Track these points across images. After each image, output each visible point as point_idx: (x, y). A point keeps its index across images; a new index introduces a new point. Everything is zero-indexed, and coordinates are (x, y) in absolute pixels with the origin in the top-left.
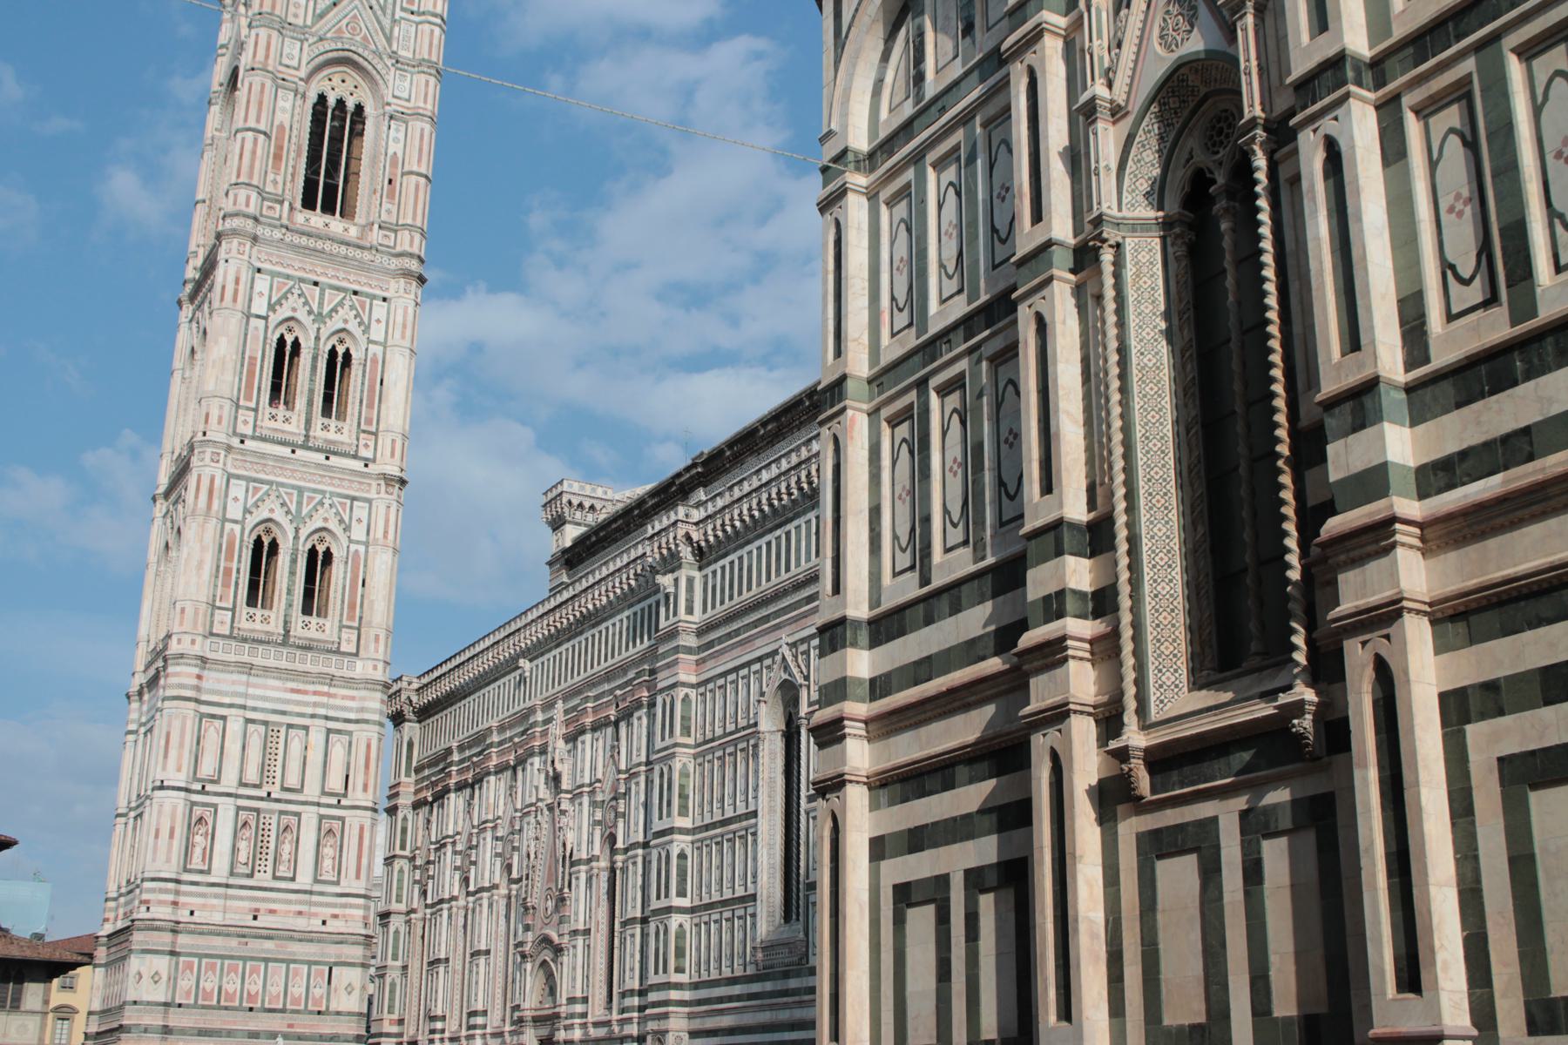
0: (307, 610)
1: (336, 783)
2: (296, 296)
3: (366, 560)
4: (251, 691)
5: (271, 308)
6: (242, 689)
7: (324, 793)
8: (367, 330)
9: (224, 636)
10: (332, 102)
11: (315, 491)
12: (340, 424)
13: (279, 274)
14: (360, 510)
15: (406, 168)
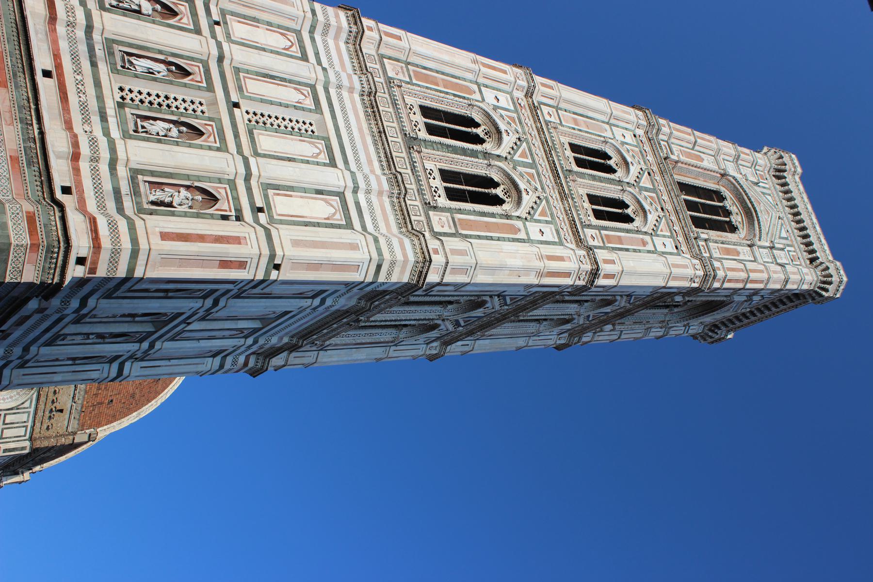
4: (345, 94)
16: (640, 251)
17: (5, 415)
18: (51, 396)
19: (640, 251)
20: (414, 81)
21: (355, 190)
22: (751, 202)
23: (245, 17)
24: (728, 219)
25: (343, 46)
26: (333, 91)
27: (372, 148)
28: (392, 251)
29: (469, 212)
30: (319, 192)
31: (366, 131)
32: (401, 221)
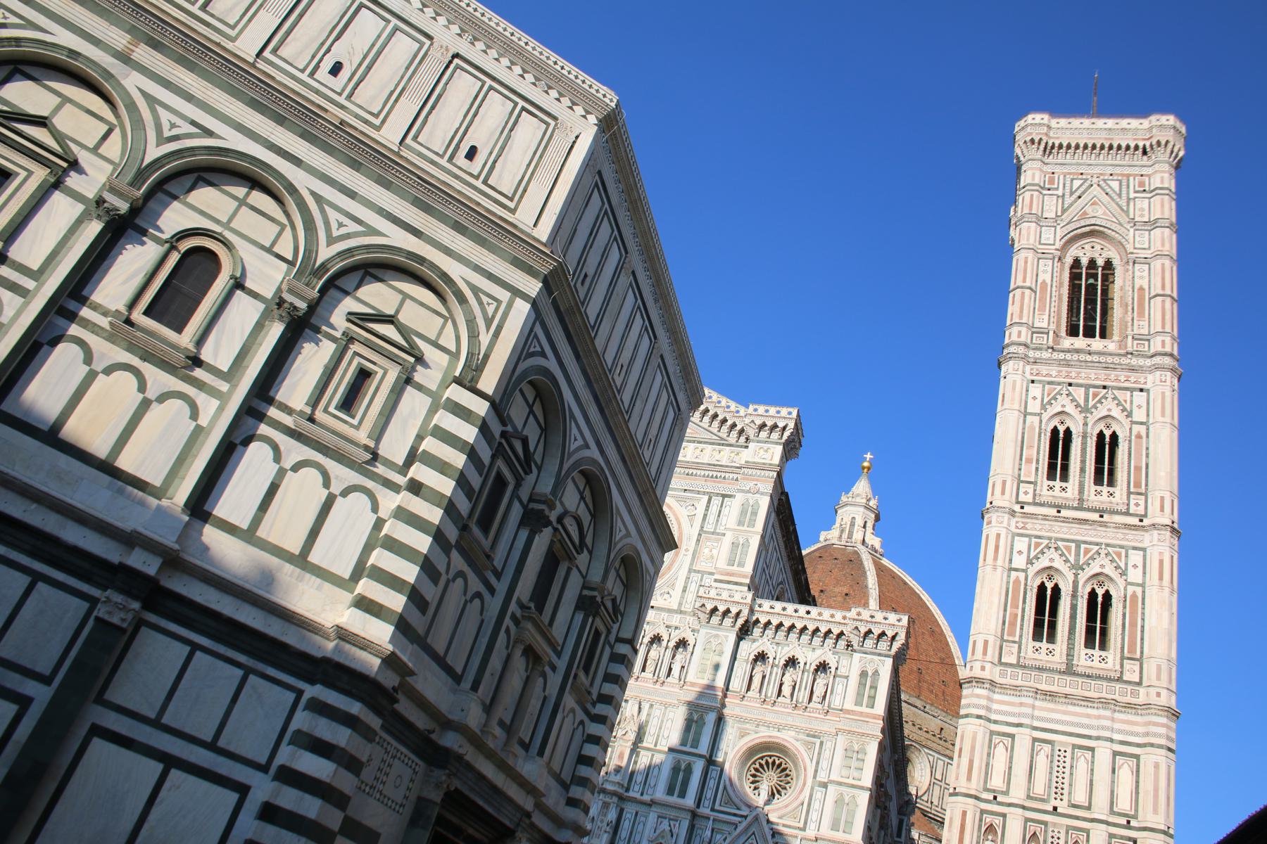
0: (1089, 643)
1: (1124, 804)
2: (1064, 396)
3: (1143, 599)
4: (1037, 713)
5: (1043, 407)
6: (1029, 711)
7: (1112, 812)
8: (1129, 415)
9: (1011, 665)
10: (1085, 262)
11: (1091, 543)
12: (1111, 490)
13: (1049, 383)
14: (1136, 557)
15: (1152, 294)
16: (1147, 449)
17: (935, 779)
18: (929, 736)
19: (1147, 449)
20: (1017, 639)
21: (1112, 740)
22: (1085, 226)
23: (987, 773)
24: (1100, 269)
25: (996, 697)
26: (1036, 724)
27: (1078, 709)
28: (1160, 736)
29: (1123, 639)
30: (1114, 771)
31: (1063, 708)
32: (1134, 711)
